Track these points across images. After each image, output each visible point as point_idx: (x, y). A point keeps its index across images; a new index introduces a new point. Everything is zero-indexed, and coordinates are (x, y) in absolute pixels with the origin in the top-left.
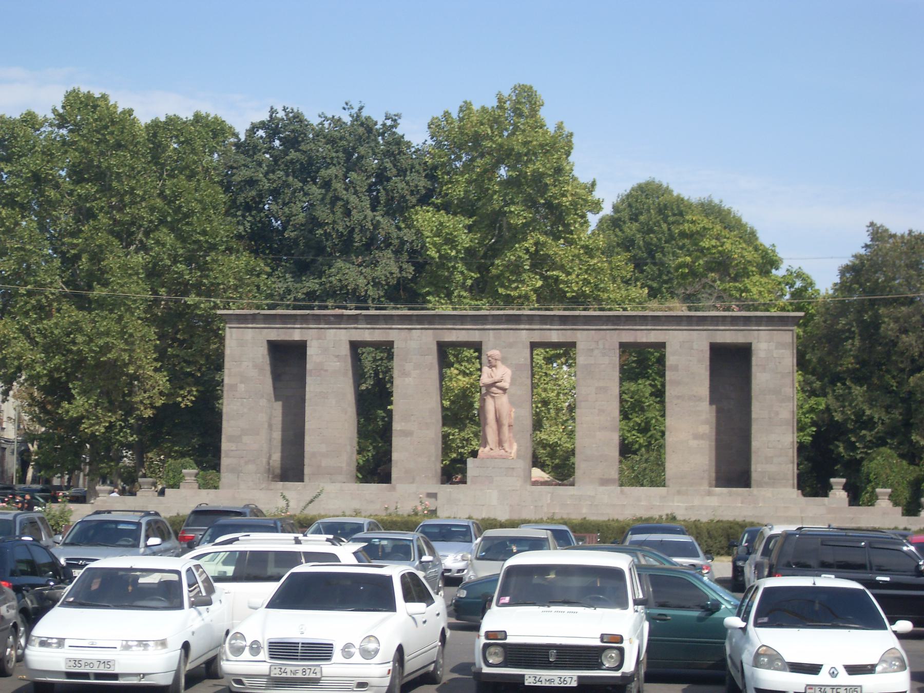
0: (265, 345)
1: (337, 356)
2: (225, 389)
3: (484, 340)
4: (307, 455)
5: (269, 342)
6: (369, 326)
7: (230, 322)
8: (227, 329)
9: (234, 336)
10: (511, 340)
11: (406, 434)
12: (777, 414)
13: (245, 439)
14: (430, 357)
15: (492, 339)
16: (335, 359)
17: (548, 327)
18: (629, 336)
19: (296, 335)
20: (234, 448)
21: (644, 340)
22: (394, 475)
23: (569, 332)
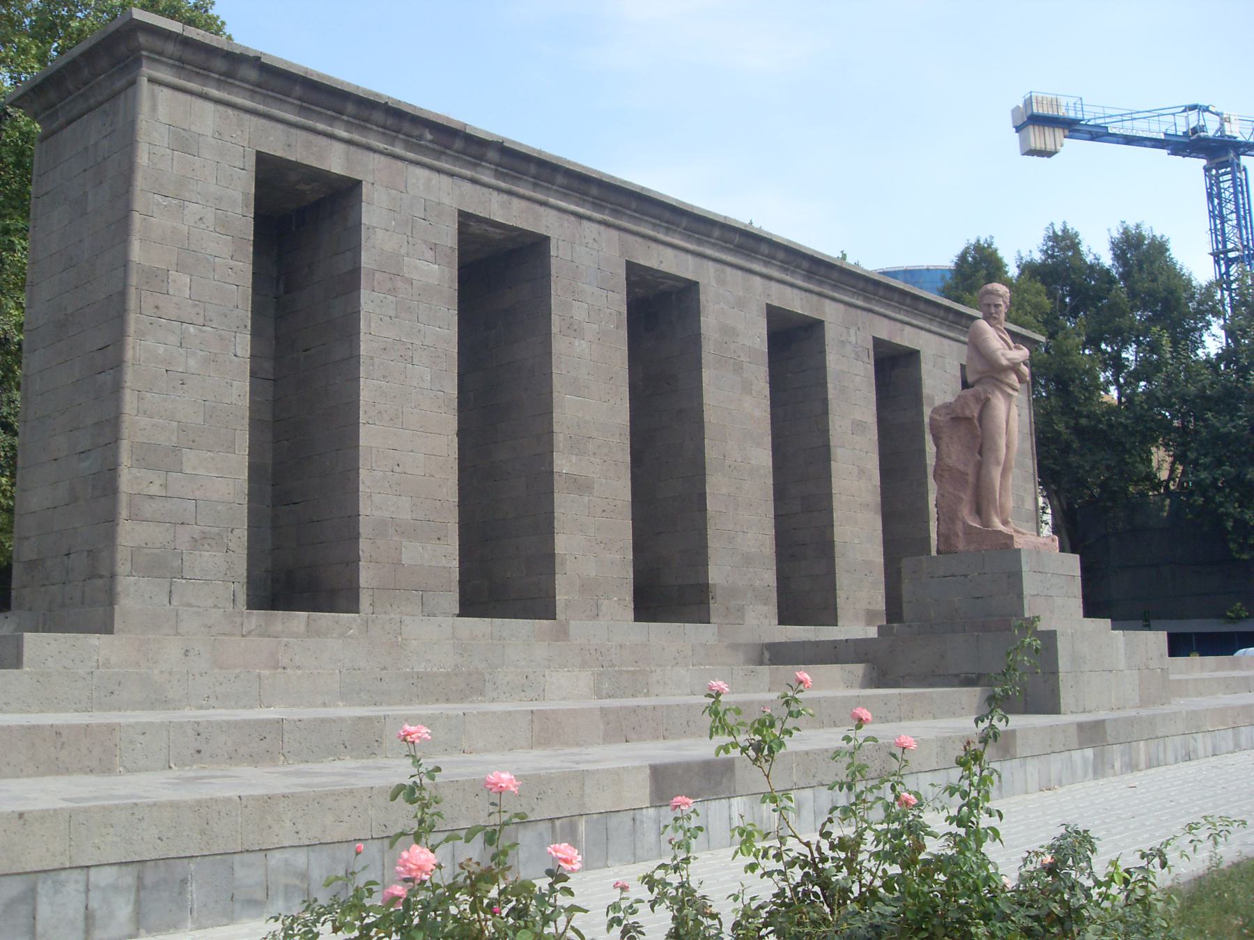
0: (251, 162)
1: (433, 247)
3: (702, 281)
6: (503, 185)
7: (158, 57)
9: (162, 111)
10: (741, 293)
11: (582, 486)
12: (1023, 502)
13: (191, 459)
14: (616, 296)
15: (713, 283)
16: (429, 255)
17: (788, 278)
18: (886, 330)
20: (155, 490)
21: (898, 340)
22: (560, 598)
23: (815, 298)
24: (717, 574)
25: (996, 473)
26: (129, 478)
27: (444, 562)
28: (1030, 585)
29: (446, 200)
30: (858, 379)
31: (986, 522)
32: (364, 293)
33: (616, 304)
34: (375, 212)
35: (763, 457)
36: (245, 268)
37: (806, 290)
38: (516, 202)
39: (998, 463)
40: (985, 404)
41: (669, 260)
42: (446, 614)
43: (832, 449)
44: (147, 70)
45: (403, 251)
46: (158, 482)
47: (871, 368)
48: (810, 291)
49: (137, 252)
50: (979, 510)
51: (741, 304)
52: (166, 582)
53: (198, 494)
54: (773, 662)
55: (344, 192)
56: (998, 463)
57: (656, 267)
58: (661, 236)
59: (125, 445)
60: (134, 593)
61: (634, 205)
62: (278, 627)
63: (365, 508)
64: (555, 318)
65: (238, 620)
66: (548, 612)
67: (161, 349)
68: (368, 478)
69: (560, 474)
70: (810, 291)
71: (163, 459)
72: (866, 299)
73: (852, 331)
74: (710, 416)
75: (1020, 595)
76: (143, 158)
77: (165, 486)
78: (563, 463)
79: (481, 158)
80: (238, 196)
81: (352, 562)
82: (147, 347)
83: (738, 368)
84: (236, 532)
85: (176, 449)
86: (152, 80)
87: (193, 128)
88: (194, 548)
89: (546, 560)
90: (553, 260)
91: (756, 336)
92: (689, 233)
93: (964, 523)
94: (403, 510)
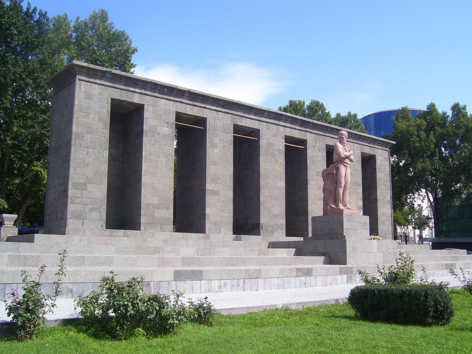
1: (167, 123)
2: (73, 136)
3: (261, 129)
4: (143, 206)
5: (113, 100)
6: (190, 102)
8: (77, 80)
9: (83, 88)
11: (216, 193)
12: (385, 197)
13: (90, 186)
15: (265, 129)
16: (166, 125)
17: (294, 126)
19: (136, 99)
20: (78, 195)
22: (207, 227)
24: (263, 220)
25: (341, 191)
26: (71, 192)
27: (168, 216)
28: (346, 225)
29: (172, 109)
30: (319, 158)
31: (337, 206)
32: (144, 138)
33: (230, 137)
34: (147, 114)
35: (282, 184)
36: (107, 132)
37: (300, 130)
38: (195, 107)
39: (341, 187)
40: (338, 169)
41: (248, 122)
42: (169, 231)
43: (308, 181)
44: (78, 77)
45: (157, 125)
46: (80, 193)
47: (325, 154)
48: (302, 130)
49: (74, 129)
50: (336, 203)
51: (275, 135)
52: (82, 221)
53: (92, 196)
54: (273, 247)
55: (140, 108)
56: (341, 187)
57: (244, 125)
58: (246, 115)
59: (70, 183)
60: (71, 224)
61: (236, 107)
62: (115, 234)
63: (143, 200)
64: (208, 143)
65: (103, 232)
66: (203, 231)
67: (81, 156)
68: (144, 191)
69: (208, 190)
70: (302, 130)
71: (82, 186)
72: (323, 132)
73: (318, 142)
74: (262, 171)
75: (343, 229)
76: (76, 102)
77: (82, 194)
78: (209, 186)
79: (184, 95)
80: (105, 111)
81: (139, 216)
82: (76, 155)
83: (273, 156)
84: (103, 207)
85: (85, 184)
86: (79, 80)
87: (92, 93)
88: (90, 211)
89: (203, 215)
90: (207, 125)
91: (281, 145)
92: (256, 114)
93: (331, 206)
94: (156, 201)
